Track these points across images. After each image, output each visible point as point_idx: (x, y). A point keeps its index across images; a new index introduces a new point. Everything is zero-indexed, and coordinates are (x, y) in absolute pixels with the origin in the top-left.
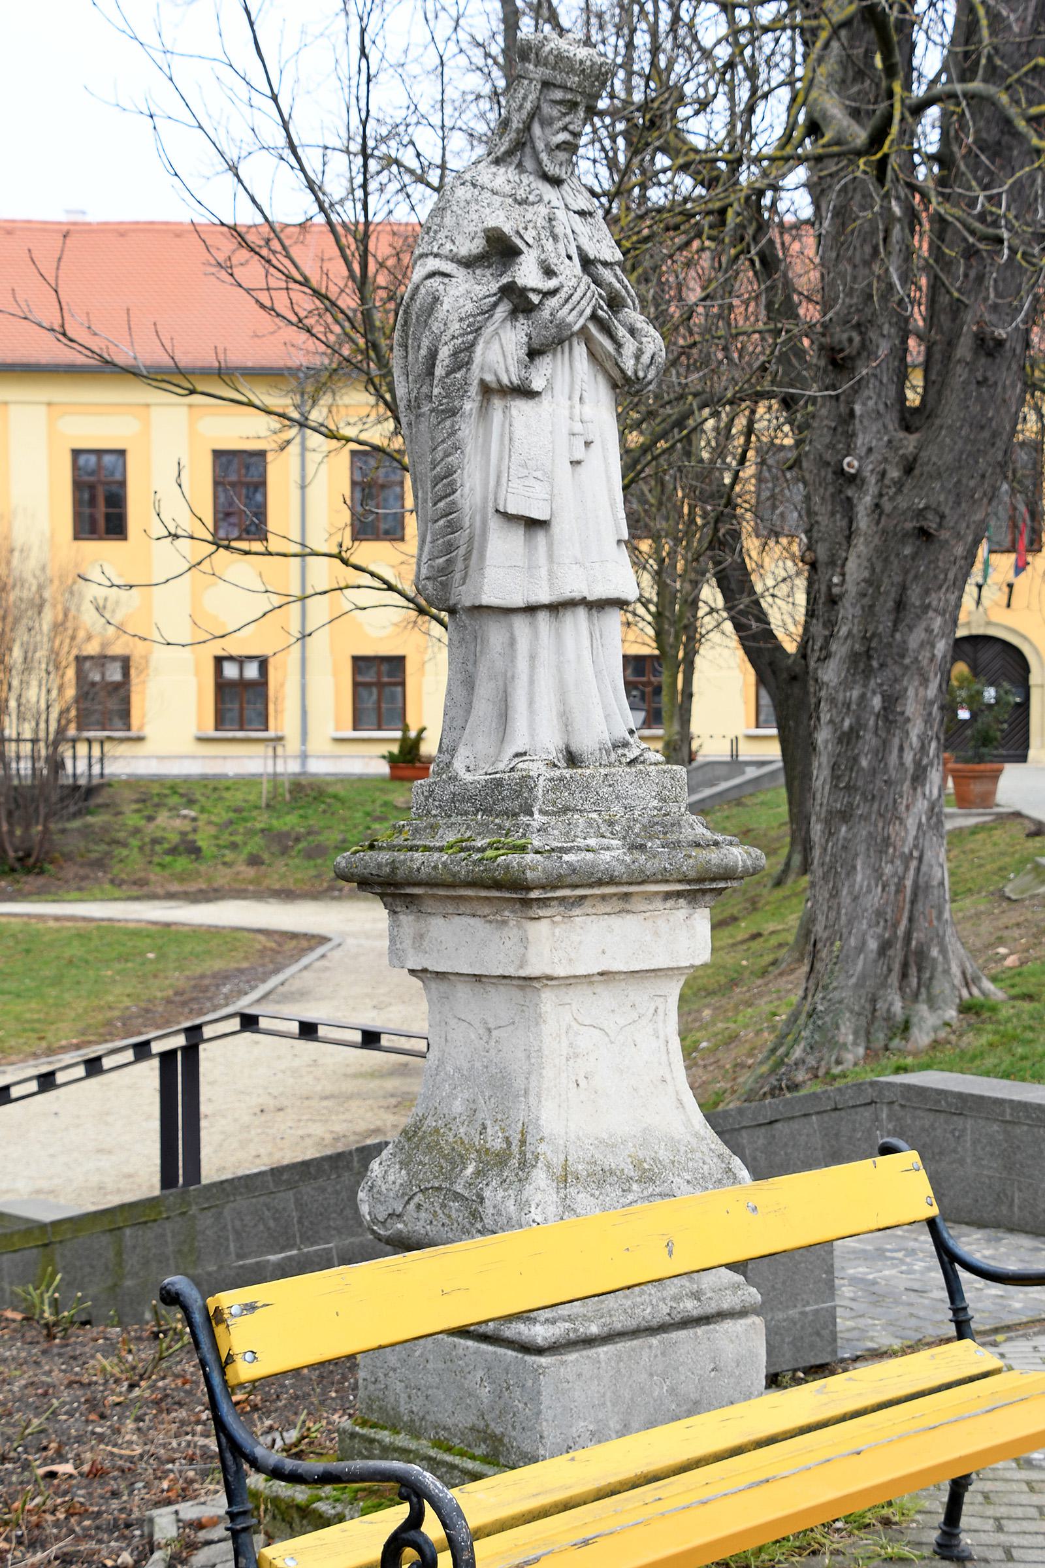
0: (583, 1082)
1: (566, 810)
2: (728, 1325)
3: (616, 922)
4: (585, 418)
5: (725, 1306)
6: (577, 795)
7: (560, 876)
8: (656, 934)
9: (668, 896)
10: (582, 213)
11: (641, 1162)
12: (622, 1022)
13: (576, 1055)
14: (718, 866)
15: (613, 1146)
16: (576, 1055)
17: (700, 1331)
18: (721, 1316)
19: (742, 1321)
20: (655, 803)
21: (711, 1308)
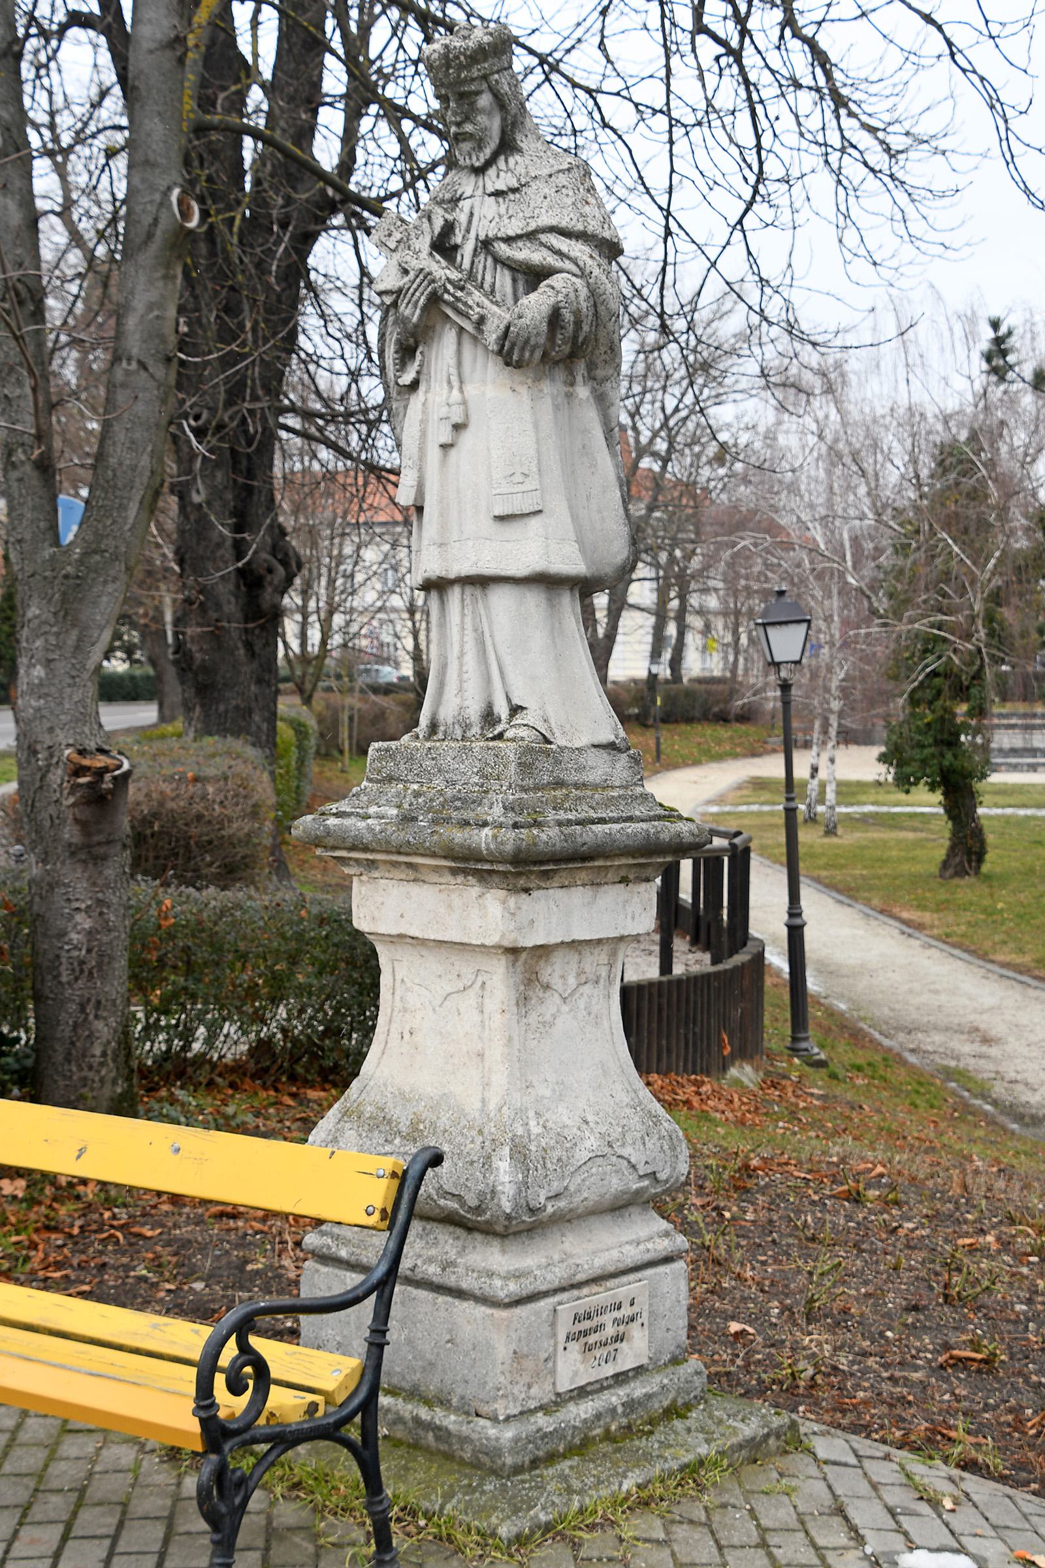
0: (407, 1036)
1: (390, 779)
2: (467, 1306)
3: (415, 889)
4: (451, 401)
5: (464, 1285)
6: (402, 767)
7: (317, 837)
8: (450, 906)
9: (454, 872)
10: (498, 194)
11: (420, 1121)
12: (449, 989)
13: (405, 1010)
14: (462, 846)
15: (409, 1100)
16: (405, 1010)
17: (442, 1299)
18: (459, 1294)
19: (483, 1308)
20: (476, 779)
21: (451, 1280)
